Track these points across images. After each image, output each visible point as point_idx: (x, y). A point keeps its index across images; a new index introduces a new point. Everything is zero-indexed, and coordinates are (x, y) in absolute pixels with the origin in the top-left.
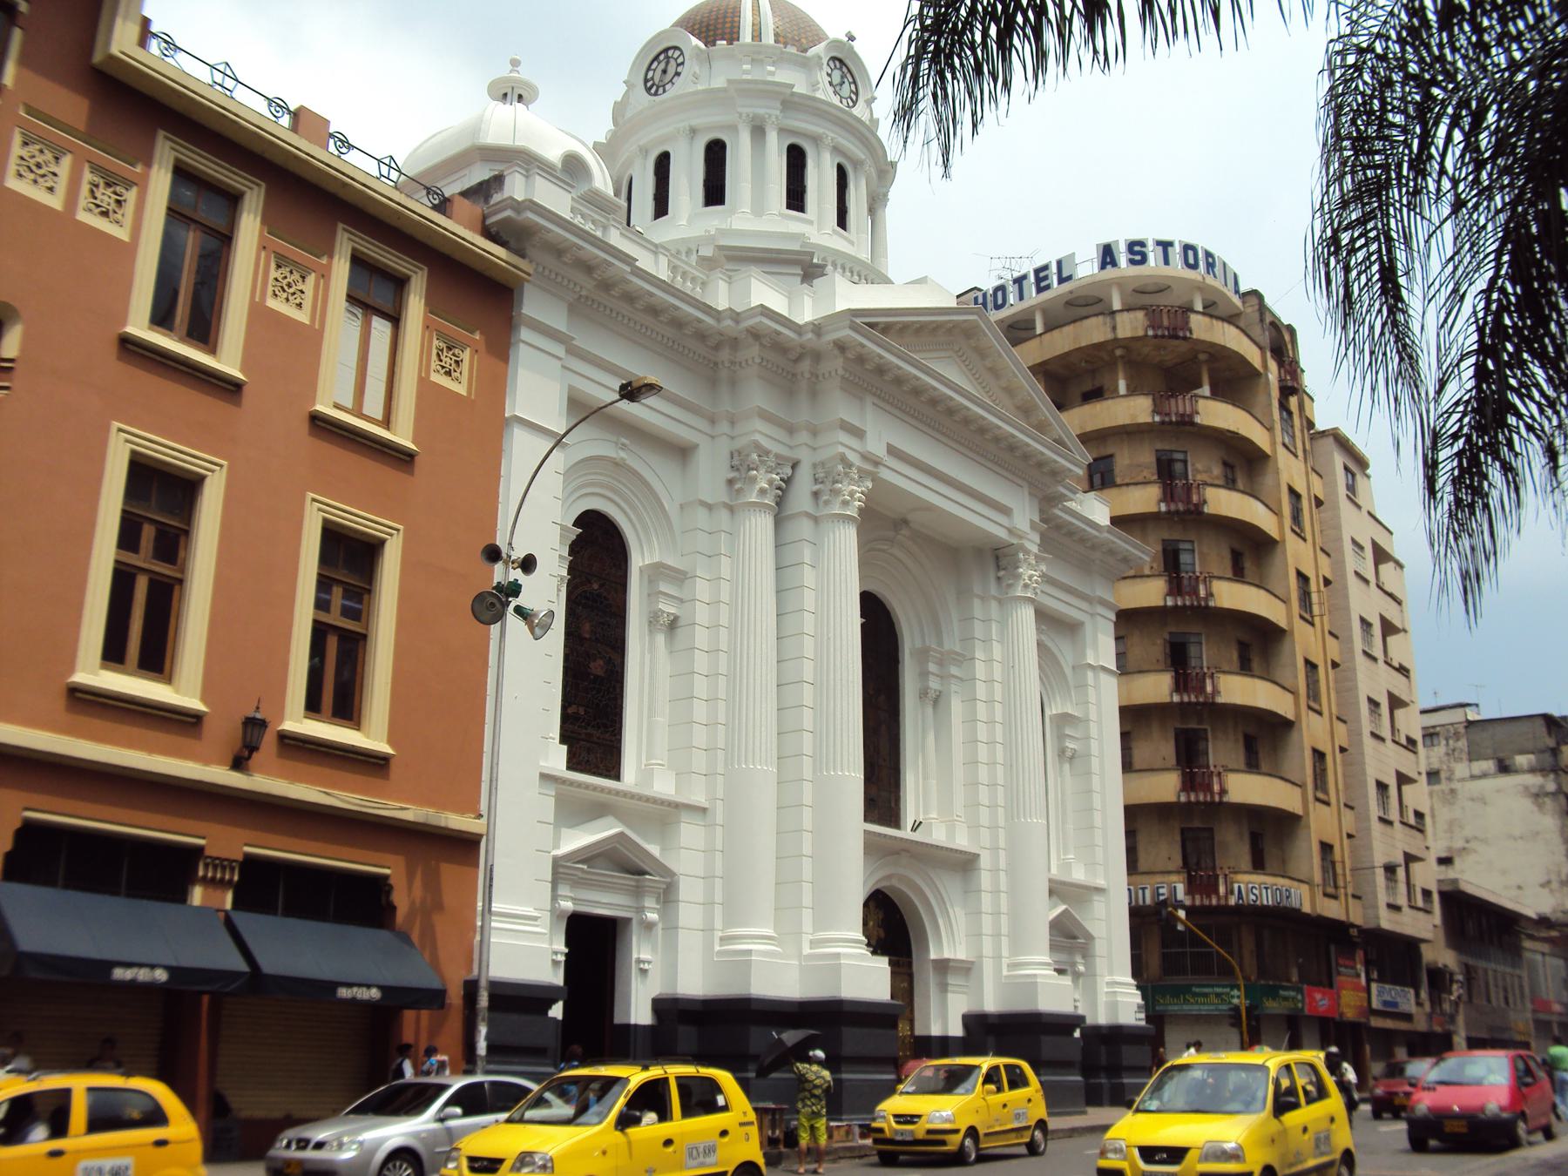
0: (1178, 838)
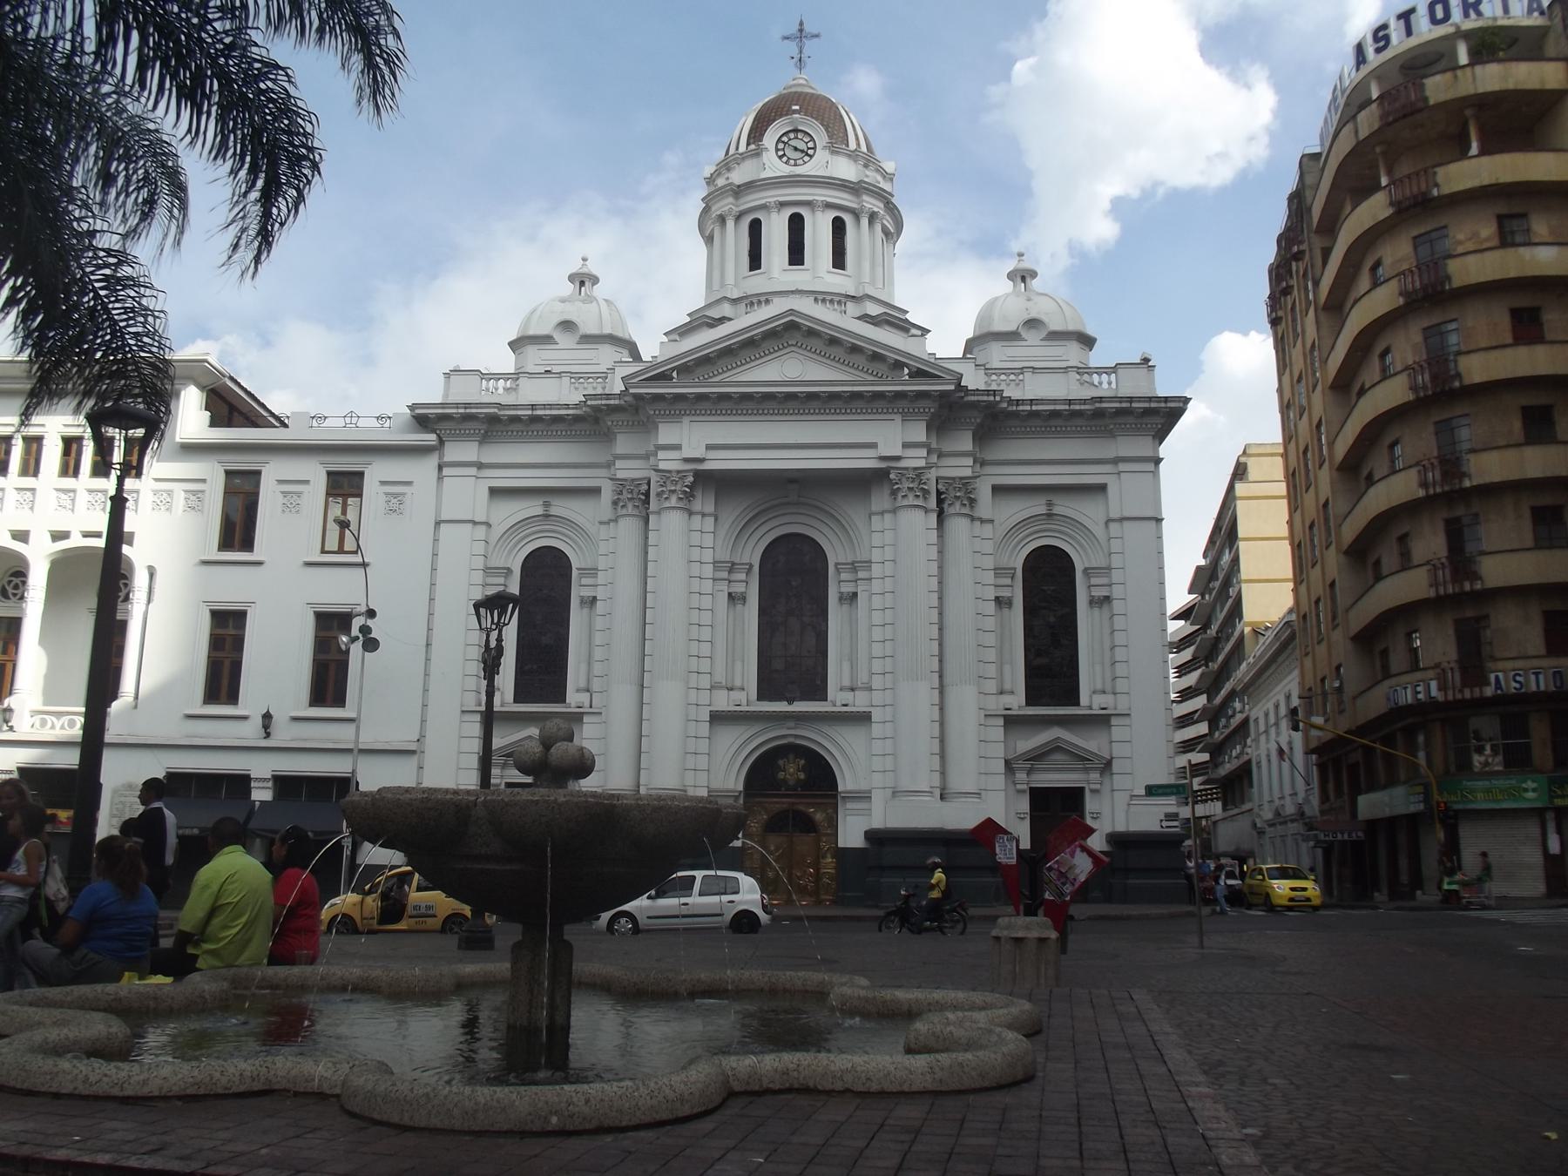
0: (1451, 631)
